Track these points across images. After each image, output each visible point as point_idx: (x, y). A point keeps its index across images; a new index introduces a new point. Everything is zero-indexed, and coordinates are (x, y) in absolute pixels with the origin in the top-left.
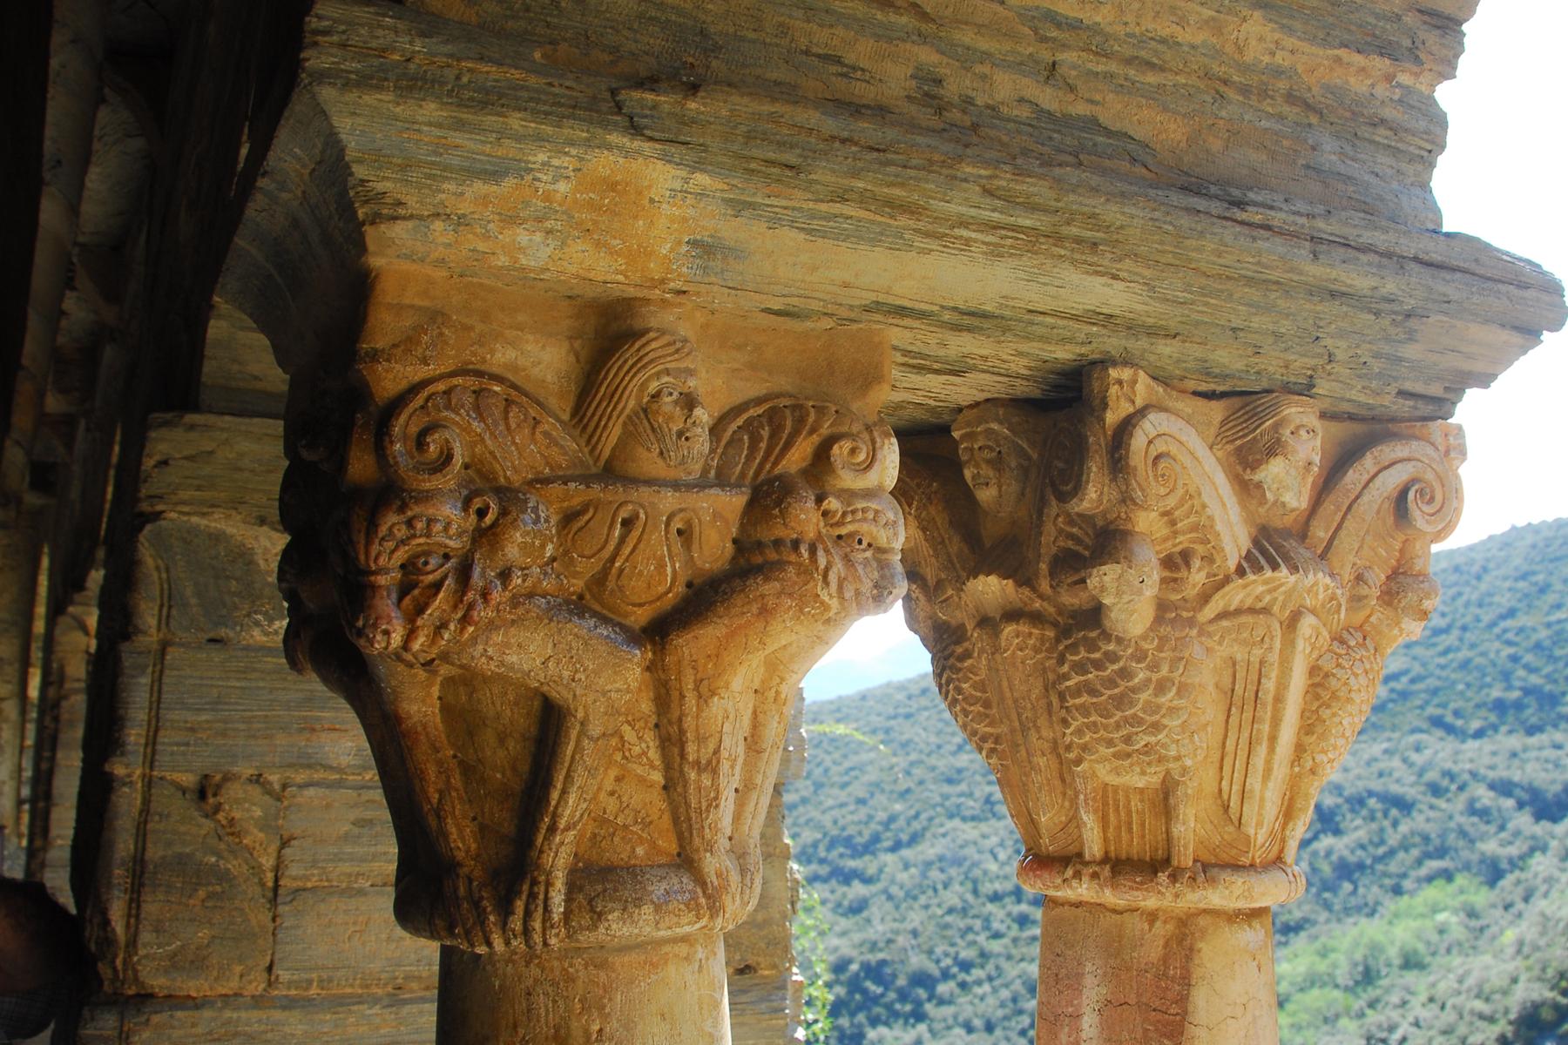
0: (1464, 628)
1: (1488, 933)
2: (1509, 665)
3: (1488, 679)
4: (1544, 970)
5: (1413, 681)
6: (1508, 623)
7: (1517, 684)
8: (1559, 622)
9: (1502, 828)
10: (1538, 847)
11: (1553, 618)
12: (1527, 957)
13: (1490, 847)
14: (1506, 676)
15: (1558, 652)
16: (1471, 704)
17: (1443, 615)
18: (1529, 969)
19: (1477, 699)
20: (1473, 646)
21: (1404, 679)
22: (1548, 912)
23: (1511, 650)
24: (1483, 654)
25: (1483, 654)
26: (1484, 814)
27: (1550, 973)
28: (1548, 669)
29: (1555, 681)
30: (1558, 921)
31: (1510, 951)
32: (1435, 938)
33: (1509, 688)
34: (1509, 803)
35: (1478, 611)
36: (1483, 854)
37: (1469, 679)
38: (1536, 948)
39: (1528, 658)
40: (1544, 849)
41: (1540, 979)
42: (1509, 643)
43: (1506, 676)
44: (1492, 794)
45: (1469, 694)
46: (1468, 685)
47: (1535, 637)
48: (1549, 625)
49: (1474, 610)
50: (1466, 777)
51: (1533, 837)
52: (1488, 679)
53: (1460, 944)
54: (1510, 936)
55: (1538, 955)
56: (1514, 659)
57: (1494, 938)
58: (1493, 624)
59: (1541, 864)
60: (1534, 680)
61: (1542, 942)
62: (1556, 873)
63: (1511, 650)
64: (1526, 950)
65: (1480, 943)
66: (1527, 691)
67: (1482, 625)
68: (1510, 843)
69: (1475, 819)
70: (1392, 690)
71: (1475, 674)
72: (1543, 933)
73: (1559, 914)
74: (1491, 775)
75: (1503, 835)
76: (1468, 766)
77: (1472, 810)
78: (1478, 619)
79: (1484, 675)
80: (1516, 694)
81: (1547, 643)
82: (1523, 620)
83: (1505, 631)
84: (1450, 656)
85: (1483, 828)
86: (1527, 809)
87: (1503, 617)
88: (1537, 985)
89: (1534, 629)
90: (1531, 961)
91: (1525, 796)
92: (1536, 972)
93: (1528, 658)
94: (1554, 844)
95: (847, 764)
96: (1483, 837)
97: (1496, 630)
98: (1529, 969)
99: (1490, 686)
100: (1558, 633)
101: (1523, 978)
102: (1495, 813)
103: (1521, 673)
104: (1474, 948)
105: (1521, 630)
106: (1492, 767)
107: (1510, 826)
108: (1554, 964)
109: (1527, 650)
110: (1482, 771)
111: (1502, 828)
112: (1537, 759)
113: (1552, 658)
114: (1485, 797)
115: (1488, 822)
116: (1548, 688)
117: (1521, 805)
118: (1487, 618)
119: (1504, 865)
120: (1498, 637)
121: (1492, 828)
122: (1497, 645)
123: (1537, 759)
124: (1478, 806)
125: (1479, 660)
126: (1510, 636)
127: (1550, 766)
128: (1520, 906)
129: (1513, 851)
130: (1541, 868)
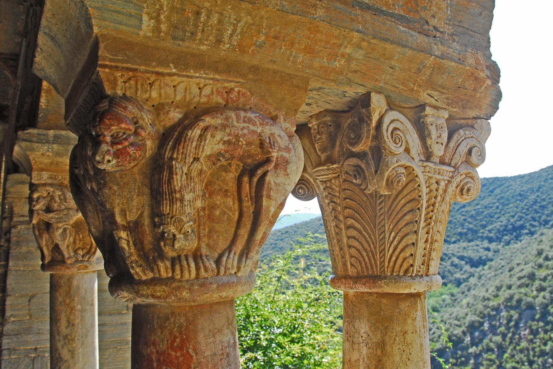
1: (457, 301)
2: (463, 222)
3: (457, 226)
4: (475, 311)
6: (463, 209)
7: (466, 227)
8: (478, 209)
9: (461, 270)
10: (472, 275)
11: (476, 208)
12: (470, 308)
13: (458, 276)
14: (462, 225)
15: (478, 218)
16: (452, 233)
18: (471, 311)
19: (454, 232)
20: (452, 216)
22: (476, 294)
23: (464, 217)
24: (456, 219)
25: (456, 219)
26: (456, 266)
27: (477, 312)
28: (475, 223)
29: (477, 226)
30: (479, 297)
31: (465, 306)
32: (442, 303)
33: (463, 229)
34: (463, 262)
35: (454, 206)
36: (456, 278)
37: (452, 226)
38: (473, 305)
39: (469, 220)
40: (473, 276)
41: (474, 314)
42: (463, 215)
43: (462, 225)
44: (458, 260)
45: (451, 230)
46: (451, 228)
47: (471, 213)
48: (475, 210)
50: (451, 255)
51: (470, 272)
52: (457, 226)
53: (449, 304)
54: (465, 302)
55: (474, 307)
56: (465, 220)
57: (459, 303)
58: (458, 210)
59: (472, 280)
60: (471, 226)
61: (475, 303)
62: (477, 283)
63: (464, 217)
64: (470, 305)
65: (455, 304)
66: (468, 229)
67: (455, 210)
68: (464, 274)
69: (453, 268)
71: (453, 225)
72: (475, 301)
73: (480, 295)
74: (458, 254)
75: (462, 272)
76: (451, 252)
77: (452, 265)
78: (454, 208)
79: (456, 225)
80: (465, 230)
81: (474, 215)
82: (468, 208)
83: (462, 212)
85: (456, 270)
86: (469, 264)
87: (462, 208)
88: (473, 316)
89: (471, 211)
90: (471, 309)
91: (468, 260)
92: (473, 312)
93: (469, 220)
94: (476, 274)
95: (263, 254)
96: (456, 273)
97: (460, 212)
98: (471, 311)
99: (457, 228)
100: (478, 212)
101: (469, 314)
102: (459, 265)
103: (467, 224)
104: (453, 305)
105: (467, 212)
106: (458, 252)
107: (464, 269)
108: (479, 310)
109: (469, 217)
110: (455, 253)
111: (461, 270)
112: (472, 249)
113: (476, 220)
114: (456, 261)
115: (457, 268)
116: (475, 228)
117: (467, 263)
118: (457, 208)
119: (462, 281)
120: (460, 214)
121: (458, 270)
122: (460, 216)
123: (472, 249)
124: (454, 263)
125: (455, 220)
126: (464, 213)
127: (475, 251)
128: (466, 293)
129: (464, 276)
130: (473, 281)
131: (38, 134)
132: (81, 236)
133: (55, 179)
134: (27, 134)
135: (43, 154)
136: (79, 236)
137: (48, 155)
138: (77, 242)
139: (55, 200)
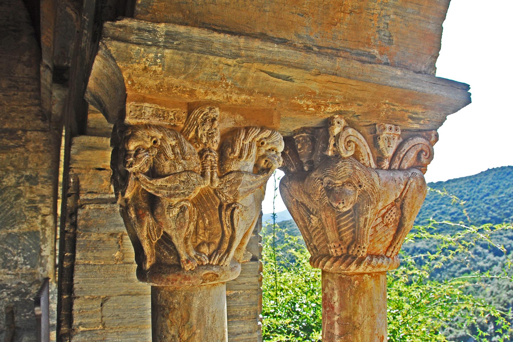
0: (474, 199)
1: (480, 289)
2: (487, 210)
3: (481, 214)
4: (499, 300)
5: (458, 215)
6: (487, 198)
7: (489, 216)
8: (502, 197)
9: (484, 258)
10: (495, 264)
11: (500, 196)
12: (494, 296)
13: (481, 264)
14: (486, 213)
15: (502, 206)
16: (475, 222)
17: (467, 195)
18: (495, 300)
19: (477, 220)
20: (476, 205)
21: (456, 214)
22: (500, 283)
23: (488, 206)
24: (479, 207)
25: (479, 207)
26: (479, 254)
27: (501, 301)
28: (499, 211)
29: (501, 215)
30: (503, 286)
31: (489, 294)
32: (465, 290)
33: (487, 217)
34: (486, 251)
35: (478, 194)
36: (479, 266)
37: (475, 214)
38: (497, 294)
39: (493, 208)
40: (497, 264)
41: (498, 303)
42: (487, 204)
43: (486, 213)
44: (482, 248)
45: (475, 219)
46: (475, 216)
47: (495, 202)
48: (499, 198)
49: (477, 194)
51: (494, 261)
52: (481, 214)
53: (472, 292)
54: (488, 290)
55: (497, 296)
56: (488, 208)
57: (482, 291)
58: (482, 198)
59: (496, 269)
60: (494, 214)
61: (499, 292)
62: (501, 271)
63: (488, 206)
64: (494, 294)
65: (478, 292)
66: (492, 218)
67: (479, 198)
68: (487, 263)
69: (476, 256)
70: (452, 218)
71: (477, 213)
72: (499, 289)
73: (503, 284)
74: (481, 242)
75: (485, 260)
77: (475, 253)
78: (478, 196)
79: (479, 213)
80: (489, 219)
81: (498, 204)
82: (492, 197)
83: (486, 200)
84: (470, 208)
85: (479, 258)
86: (492, 253)
87: (485, 196)
88: (497, 305)
89: (494, 200)
90: (495, 298)
91: (491, 249)
92: (497, 301)
93: (493, 208)
94: (500, 263)
96: (479, 261)
97: (483, 200)
98: (495, 300)
99: (481, 216)
100: (502, 201)
101: (493, 302)
102: (482, 254)
103: (491, 212)
104: (476, 293)
105: (491, 200)
107: (487, 257)
108: (503, 299)
109: (492, 206)
110: (479, 241)
111: (484, 258)
112: (495, 238)
113: (500, 208)
114: (480, 249)
115: (480, 257)
116: (499, 217)
117: (490, 252)
118: (480, 196)
119: (485, 269)
120: (484, 202)
121: (481, 258)
122: (483, 204)
123: (495, 238)
124: (477, 251)
125: (478, 209)
126: (487, 201)
127: (499, 240)
128: (490, 281)
129: (488, 265)
130: (496, 270)
131: (139, 29)
132: (207, 221)
133: (164, 117)
134: (120, 27)
135: (145, 69)
136: (204, 221)
137: (155, 71)
138: (201, 232)
139: (165, 155)
